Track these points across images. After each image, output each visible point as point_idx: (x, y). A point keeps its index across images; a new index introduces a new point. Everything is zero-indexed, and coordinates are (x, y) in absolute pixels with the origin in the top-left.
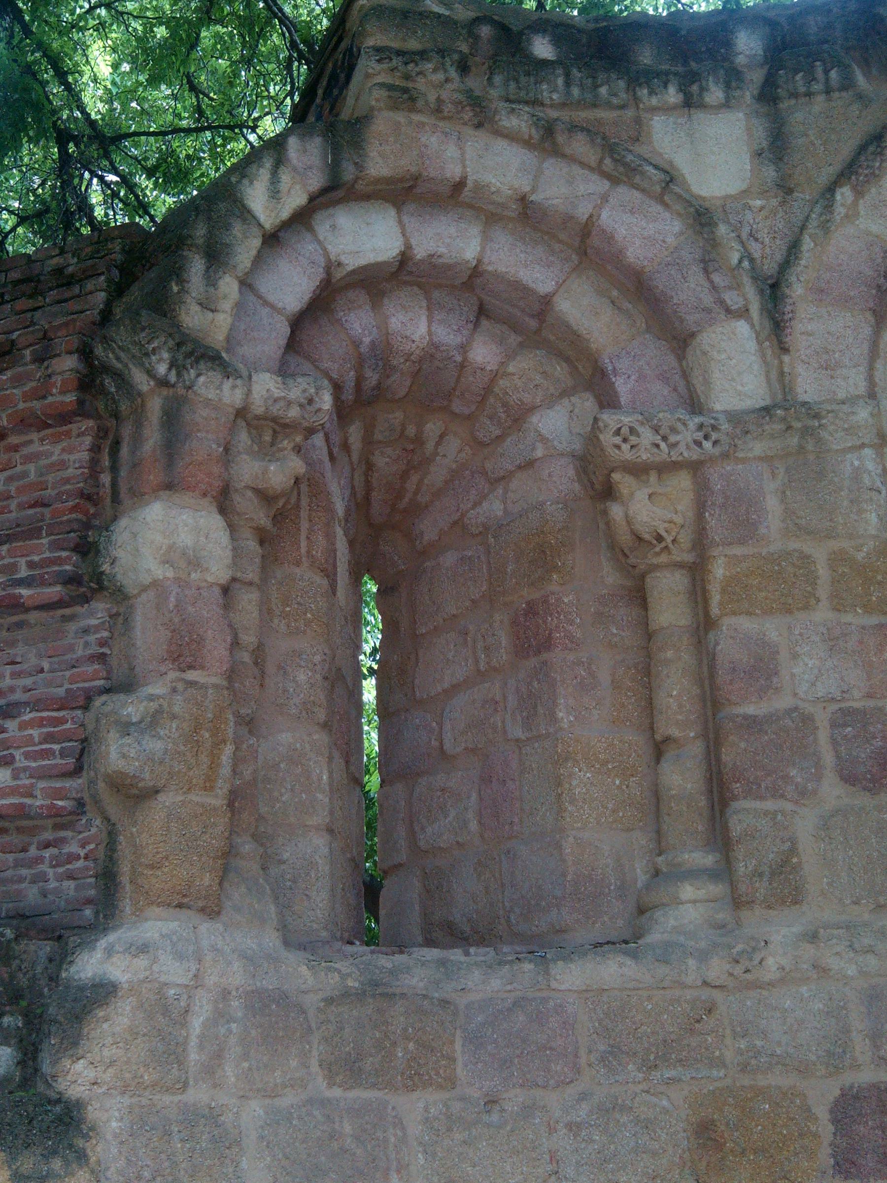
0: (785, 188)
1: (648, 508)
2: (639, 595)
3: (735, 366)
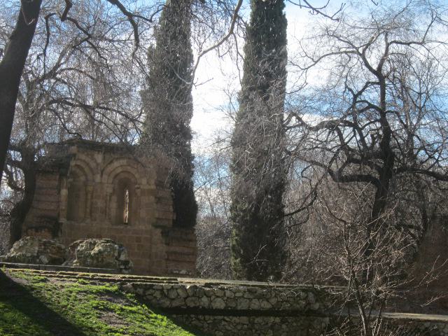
0: (104, 163)
1: (90, 189)
2: (87, 194)
3: (98, 178)
